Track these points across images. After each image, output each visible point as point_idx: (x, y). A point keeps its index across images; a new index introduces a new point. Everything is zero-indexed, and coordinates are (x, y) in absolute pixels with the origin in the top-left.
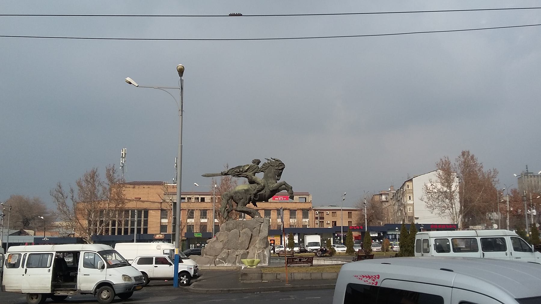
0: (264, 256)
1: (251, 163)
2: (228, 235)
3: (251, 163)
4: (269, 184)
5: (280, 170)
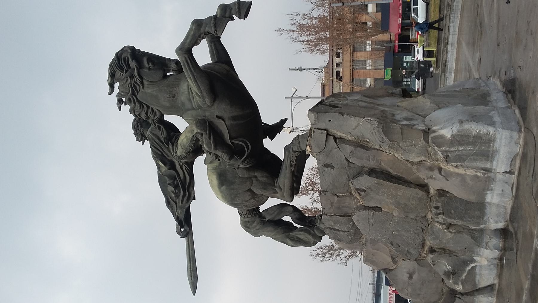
0: (460, 139)
1: (147, 143)
2: (373, 242)
3: (147, 143)
4: (195, 105)
5: (140, 66)
